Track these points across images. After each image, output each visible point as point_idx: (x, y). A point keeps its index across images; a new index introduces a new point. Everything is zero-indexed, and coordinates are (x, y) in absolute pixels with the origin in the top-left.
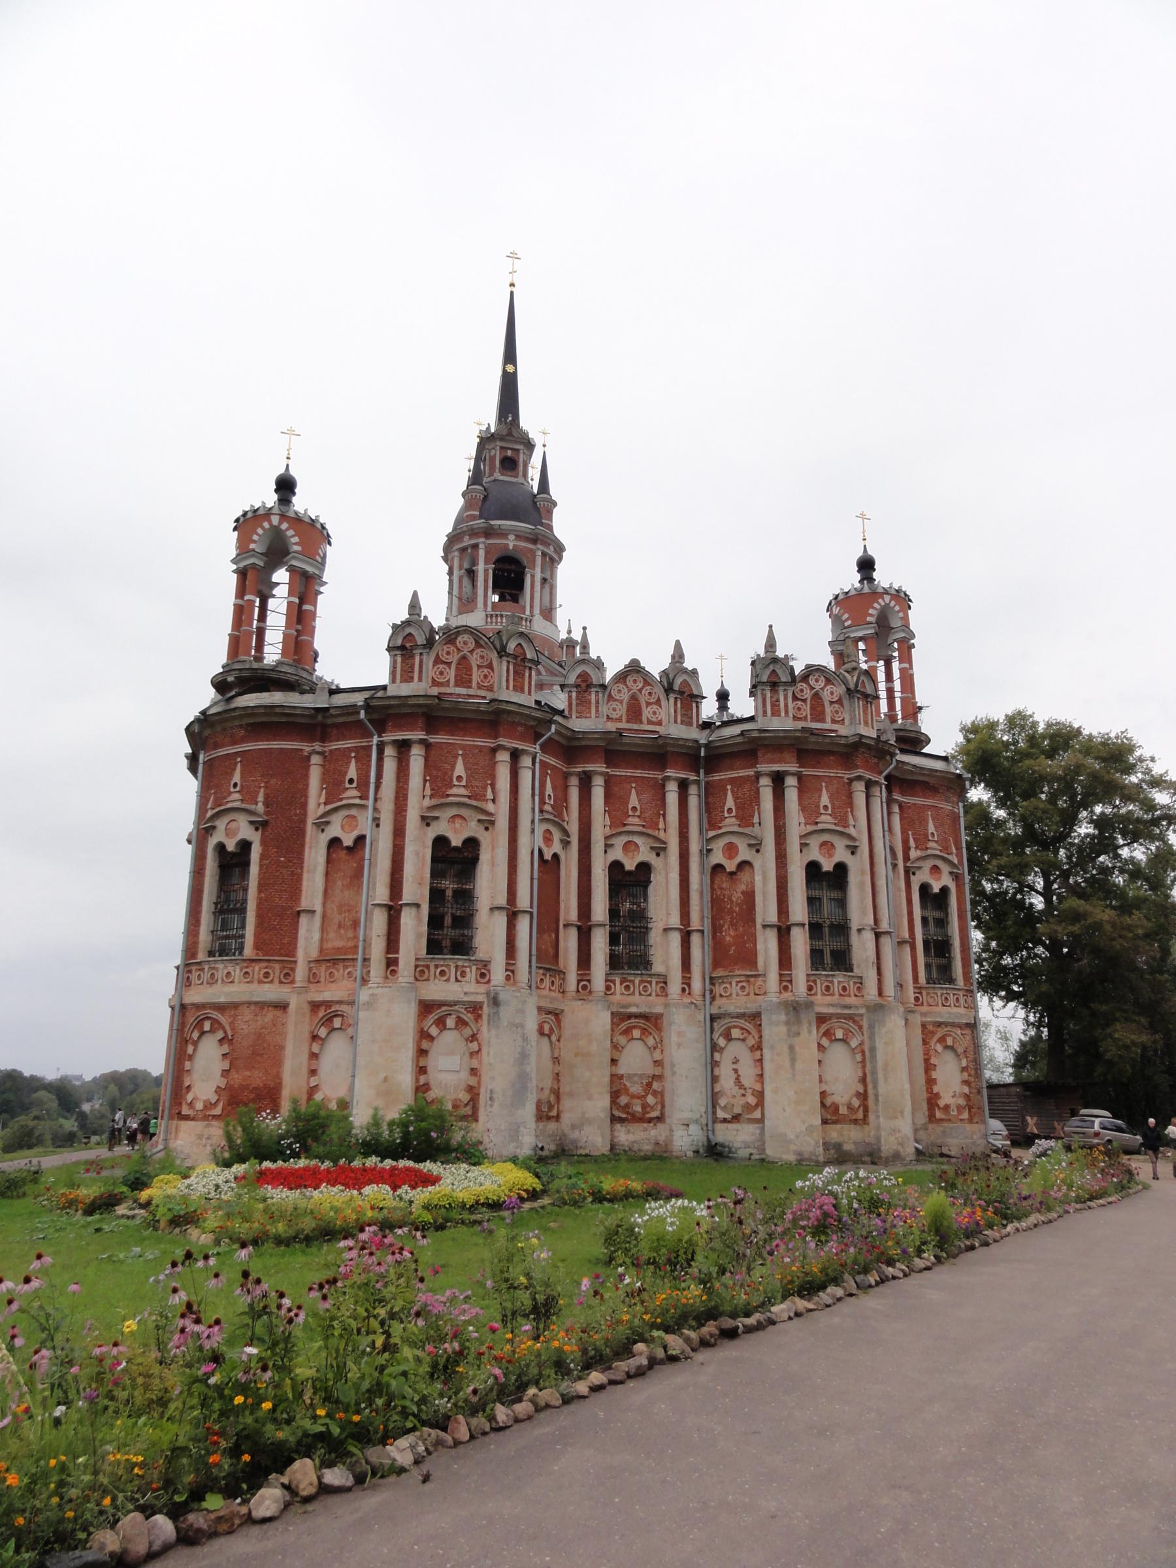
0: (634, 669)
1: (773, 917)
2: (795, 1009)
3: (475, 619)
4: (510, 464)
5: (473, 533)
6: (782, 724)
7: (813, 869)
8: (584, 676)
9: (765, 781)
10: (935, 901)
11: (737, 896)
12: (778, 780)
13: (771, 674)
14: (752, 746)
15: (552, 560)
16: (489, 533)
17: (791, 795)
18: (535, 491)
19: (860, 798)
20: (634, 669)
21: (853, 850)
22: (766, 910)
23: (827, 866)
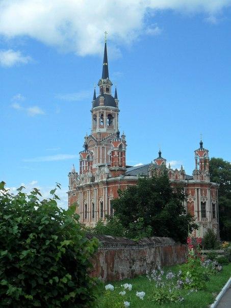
0: (176, 170)
1: (197, 210)
2: (200, 223)
3: (104, 130)
4: (108, 90)
5: (103, 109)
6: (199, 181)
7: (202, 202)
8: (170, 172)
9: (196, 190)
10: (214, 205)
11: (191, 206)
12: (198, 189)
13: (196, 173)
14: (194, 185)
15: (118, 114)
16: (106, 109)
17: (199, 192)
18: (114, 97)
19: (208, 192)
20: (176, 170)
21: (207, 200)
22: (196, 209)
23: (204, 202)
